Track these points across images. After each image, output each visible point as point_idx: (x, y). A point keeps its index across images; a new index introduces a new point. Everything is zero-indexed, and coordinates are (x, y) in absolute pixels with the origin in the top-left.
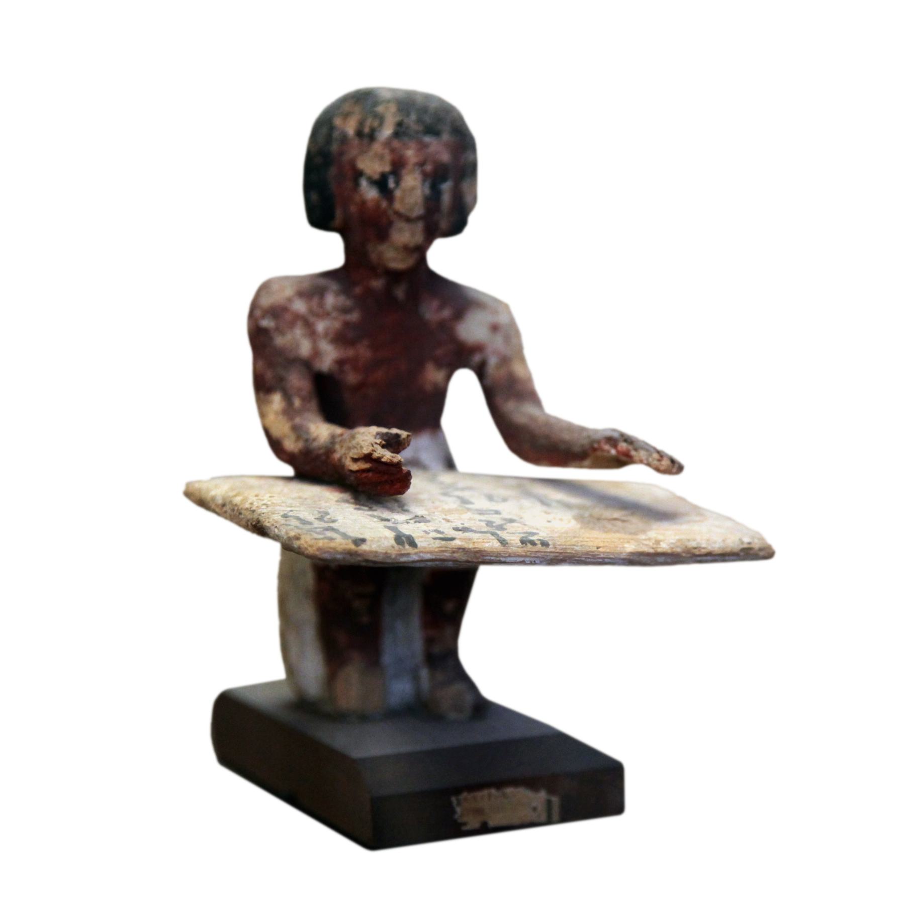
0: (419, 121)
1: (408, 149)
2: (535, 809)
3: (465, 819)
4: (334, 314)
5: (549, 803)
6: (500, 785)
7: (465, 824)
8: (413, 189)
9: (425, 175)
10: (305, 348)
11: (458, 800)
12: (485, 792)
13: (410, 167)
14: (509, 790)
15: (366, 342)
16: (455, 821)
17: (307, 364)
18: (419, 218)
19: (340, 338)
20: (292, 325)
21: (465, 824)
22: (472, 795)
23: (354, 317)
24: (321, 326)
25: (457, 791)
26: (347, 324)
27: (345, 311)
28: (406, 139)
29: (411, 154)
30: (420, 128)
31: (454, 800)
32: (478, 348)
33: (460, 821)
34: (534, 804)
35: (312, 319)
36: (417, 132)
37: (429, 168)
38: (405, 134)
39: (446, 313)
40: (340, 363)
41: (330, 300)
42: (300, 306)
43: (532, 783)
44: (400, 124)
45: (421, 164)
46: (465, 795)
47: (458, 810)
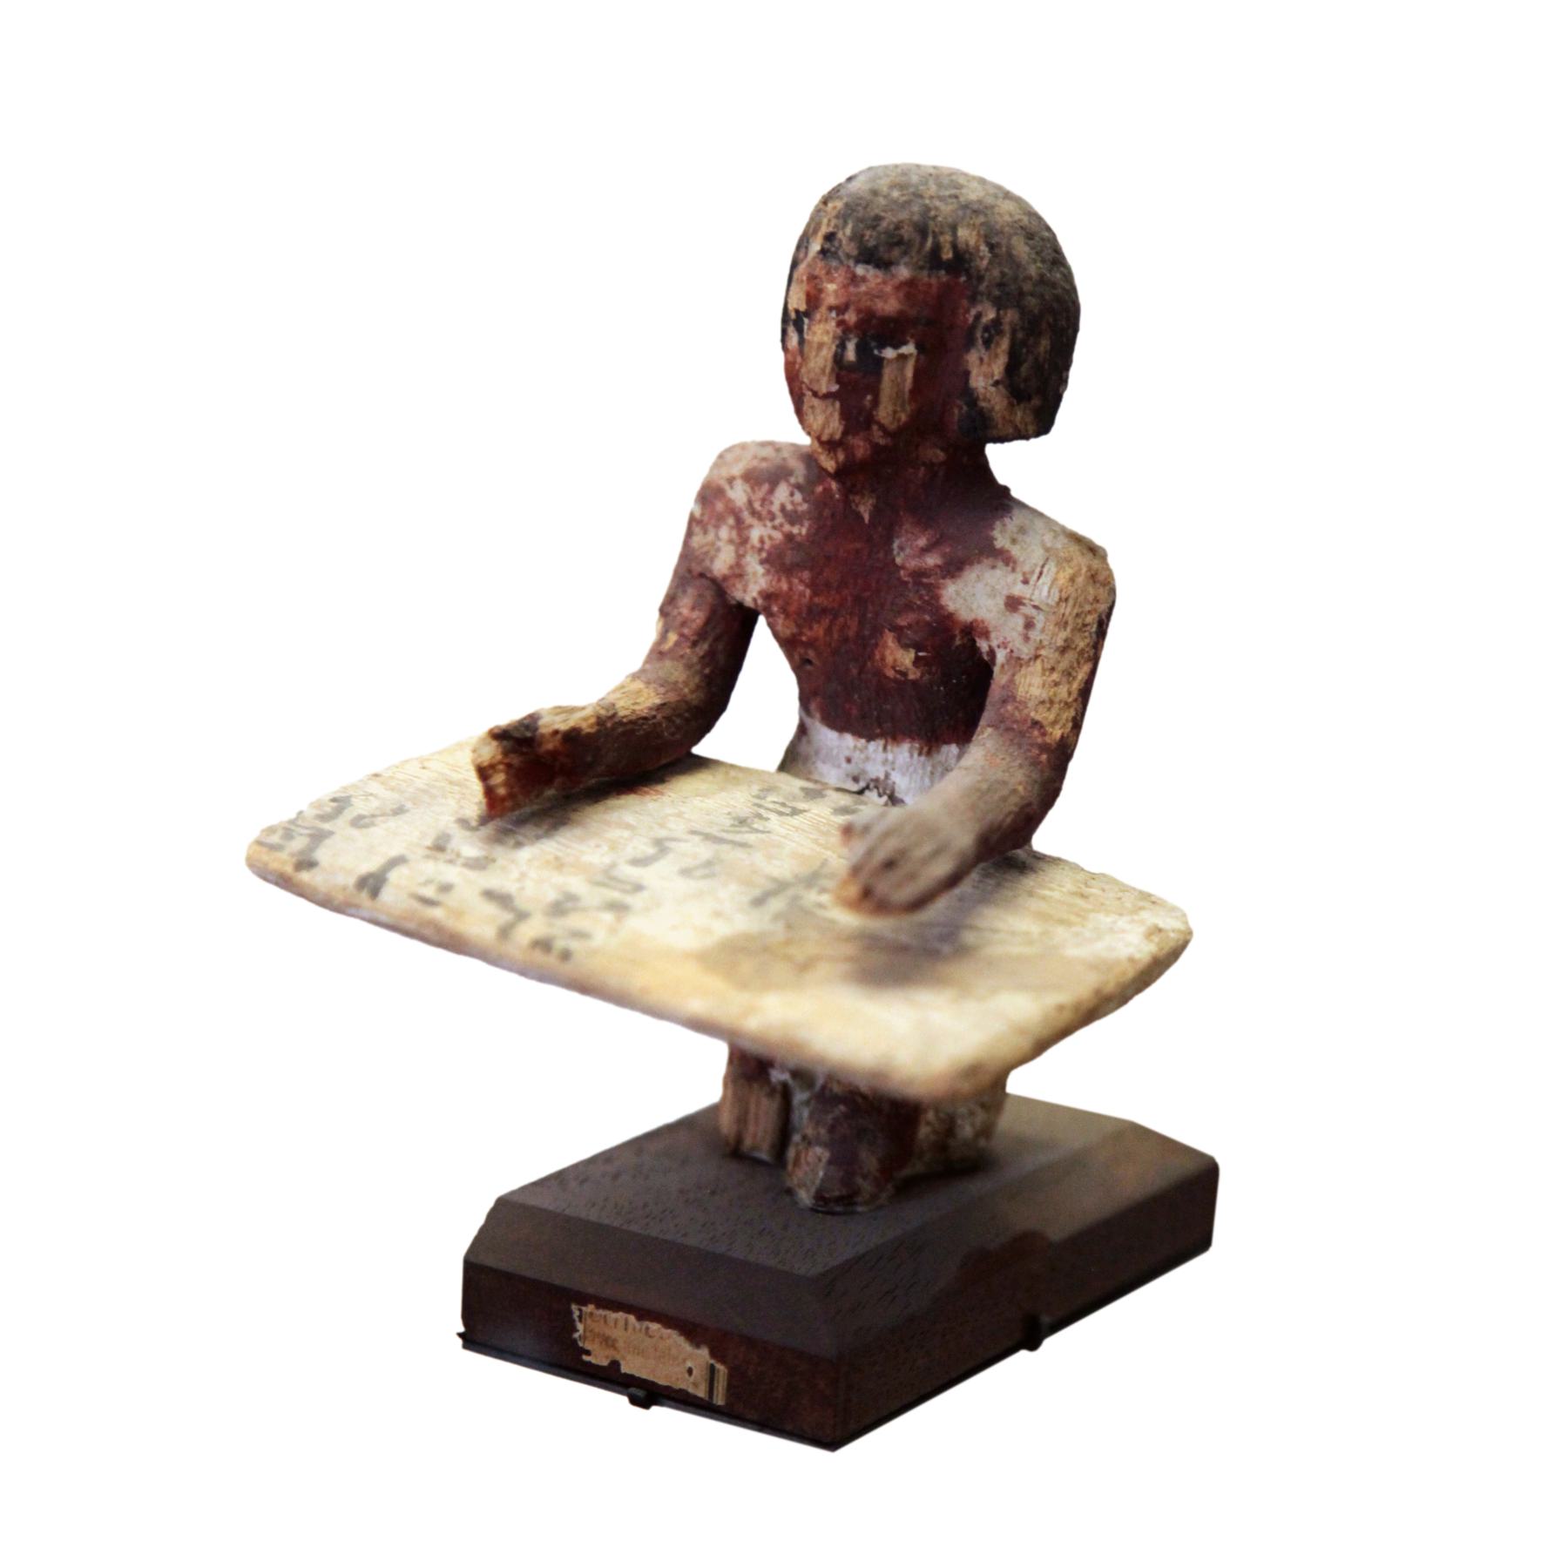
0: (857, 237)
1: (832, 281)
2: (690, 1371)
3: (588, 1346)
4: (779, 520)
5: (712, 1369)
6: (643, 1314)
7: (588, 1353)
8: (821, 345)
9: (845, 329)
10: (721, 564)
11: (580, 1310)
12: (620, 1315)
13: (823, 309)
14: (655, 1326)
15: (806, 575)
16: (575, 1342)
17: (719, 588)
18: (828, 396)
19: (775, 560)
20: (720, 519)
21: (588, 1353)
22: (601, 1312)
23: (801, 530)
24: (757, 533)
25: (583, 1300)
26: (789, 537)
27: (793, 517)
28: (834, 263)
29: (832, 290)
30: (849, 248)
31: (574, 1307)
32: (972, 631)
33: (581, 1344)
34: (689, 1364)
35: (746, 515)
36: (848, 256)
37: (851, 317)
38: (835, 255)
39: (932, 560)
40: (768, 596)
41: (782, 494)
42: (739, 494)
43: (692, 1332)
44: (830, 237)
45: (841, 309)
46: (590, 1308)
47: (580, 1327)
